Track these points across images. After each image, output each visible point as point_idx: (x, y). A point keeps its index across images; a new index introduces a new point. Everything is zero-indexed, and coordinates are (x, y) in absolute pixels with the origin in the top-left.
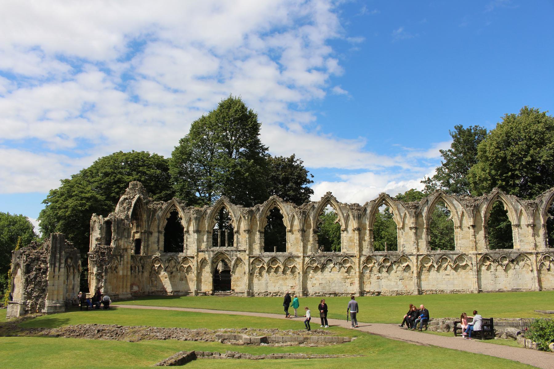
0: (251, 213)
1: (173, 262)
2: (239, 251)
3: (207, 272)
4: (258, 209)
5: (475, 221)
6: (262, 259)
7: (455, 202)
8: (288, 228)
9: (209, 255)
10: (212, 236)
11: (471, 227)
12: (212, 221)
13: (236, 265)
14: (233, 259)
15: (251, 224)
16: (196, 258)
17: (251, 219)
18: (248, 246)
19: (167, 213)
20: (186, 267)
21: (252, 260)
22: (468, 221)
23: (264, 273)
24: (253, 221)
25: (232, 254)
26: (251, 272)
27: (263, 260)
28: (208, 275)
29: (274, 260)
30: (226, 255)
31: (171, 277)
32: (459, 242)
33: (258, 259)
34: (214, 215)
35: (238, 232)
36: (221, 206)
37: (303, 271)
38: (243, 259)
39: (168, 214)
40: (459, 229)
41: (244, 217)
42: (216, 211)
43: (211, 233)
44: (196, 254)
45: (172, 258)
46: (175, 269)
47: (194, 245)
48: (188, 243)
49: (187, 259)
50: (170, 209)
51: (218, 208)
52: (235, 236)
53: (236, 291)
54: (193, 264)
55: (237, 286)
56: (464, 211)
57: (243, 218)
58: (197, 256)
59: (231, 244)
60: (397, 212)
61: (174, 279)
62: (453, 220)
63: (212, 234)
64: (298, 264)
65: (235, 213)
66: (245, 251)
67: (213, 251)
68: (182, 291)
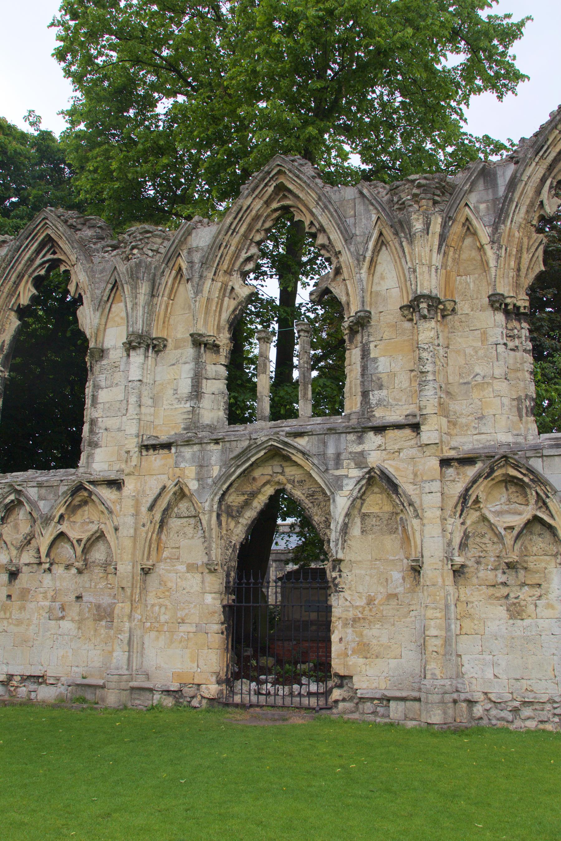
1: (21, 515)
2: (380, 429)
3: (191, 568)
6: (531, 471)
10: (224, 372)
12: (224, 286)
13: (358, 520)
14: (338, 484)
15: (444, 265)
17: (443, 238)
19: (17, 284)
20: (79, 541)
24: (458, 250)
25: (331, 451)
26: (459, 560)
27: (538, 479)
30: (298, 458)
31: (9, 596)
34: (236, 255)
36: (275, 205)
38: (399, 480)
39: (21, 288)
42: (245, 236)
43: (215, 348)
45: (19, 492)
46: (27, 557)
49: (91, 493)
50: (31, 260)
51: (257, 218)
61: (22, 608)
63: (223, 357)
65: (350, 221)
66: (416, 427)
68: (58, 679)
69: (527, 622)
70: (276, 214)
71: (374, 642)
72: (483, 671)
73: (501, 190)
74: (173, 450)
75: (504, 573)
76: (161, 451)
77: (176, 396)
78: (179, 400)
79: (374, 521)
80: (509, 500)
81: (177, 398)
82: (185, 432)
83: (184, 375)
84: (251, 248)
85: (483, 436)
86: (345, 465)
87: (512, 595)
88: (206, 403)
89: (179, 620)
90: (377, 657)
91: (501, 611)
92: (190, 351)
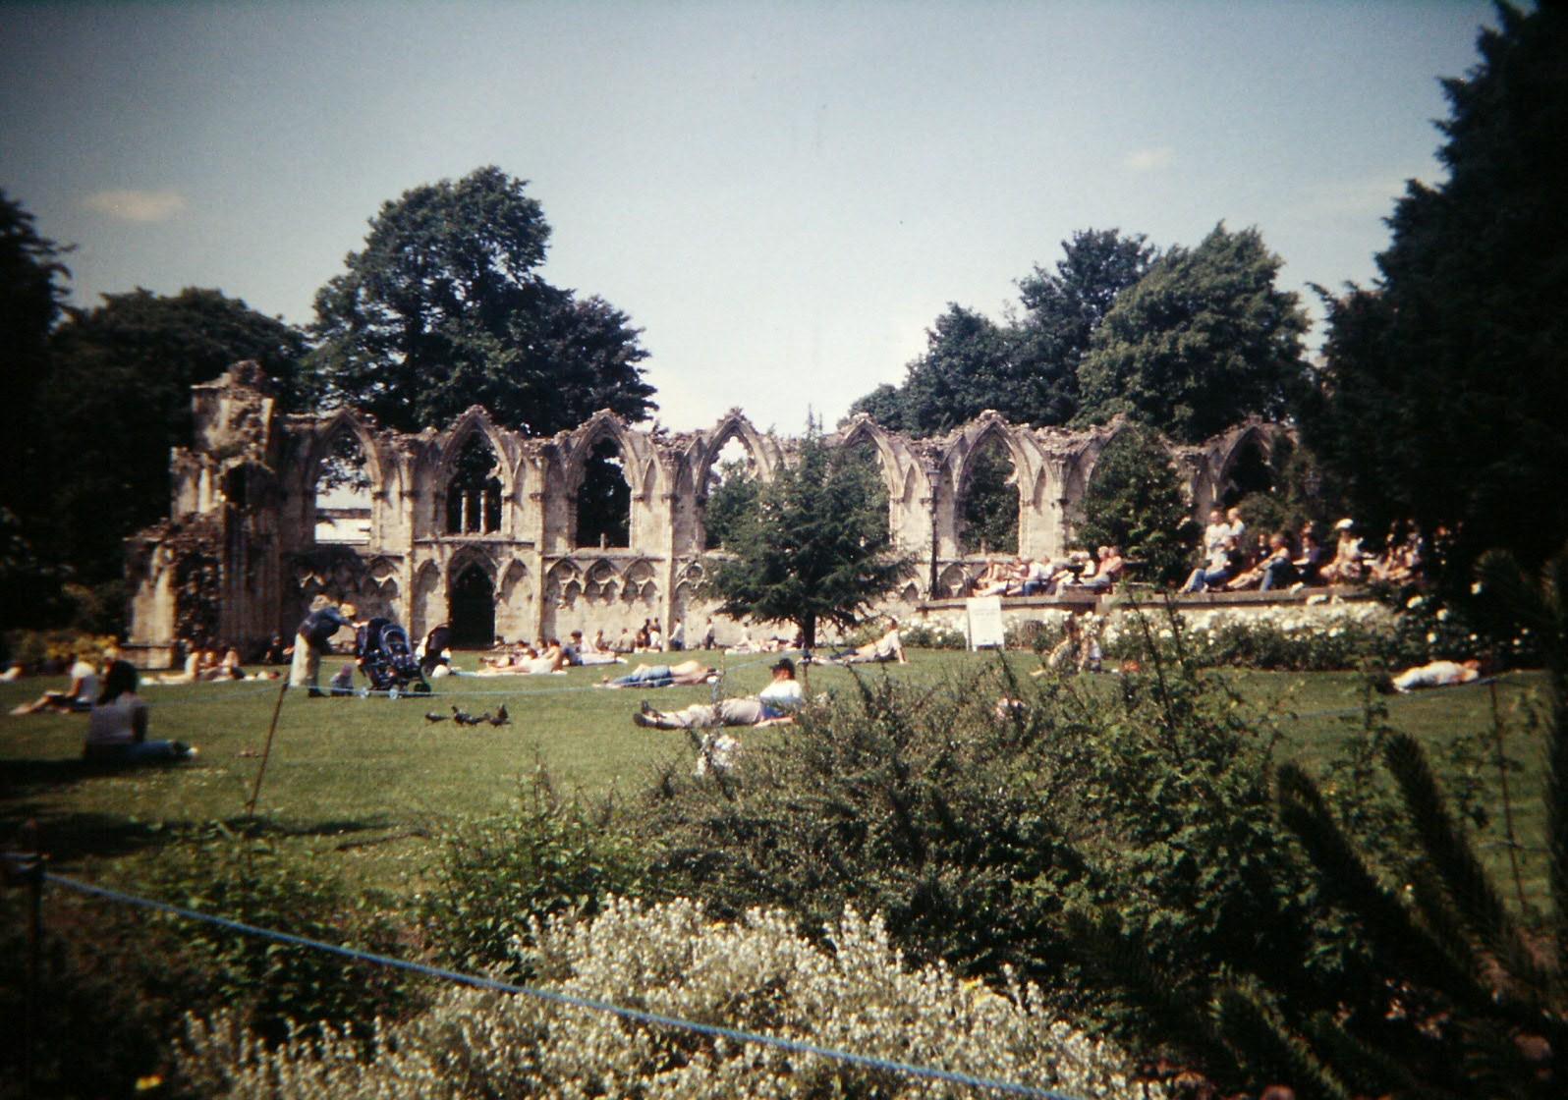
0: (549, 452)
4: (567, 444)
5: (1065, 492)
7: (1028, 447)
8: (636, 491)
9: (442, 553)
11: (1057, 504)
14: (500, 564)
16: (407, 560)
18: (540, 532)
21: (549, 567)
22: (1054, 490)
23: (579, 602)
27: (576, 568)
29: (603, 566)
32: (1029, 536)
33: (566, 565)
35: (514, 498)
37: (671, 594)
40: (1031, 508)
41: (533, 462)
44: (409, 550)
47: (401, 528)
48: (384, 522)
52: (506, 509)
53: (507, 640)
54: (402, 577)
55: (510, 627)
56: (1046, 467)
57: (528, 465)
58: (412, 555)
59: (494, 523)
60: (893, 461)
62: (1020, 486)
64: (662, 581)
67: (452, 544)
92: (431, 500)
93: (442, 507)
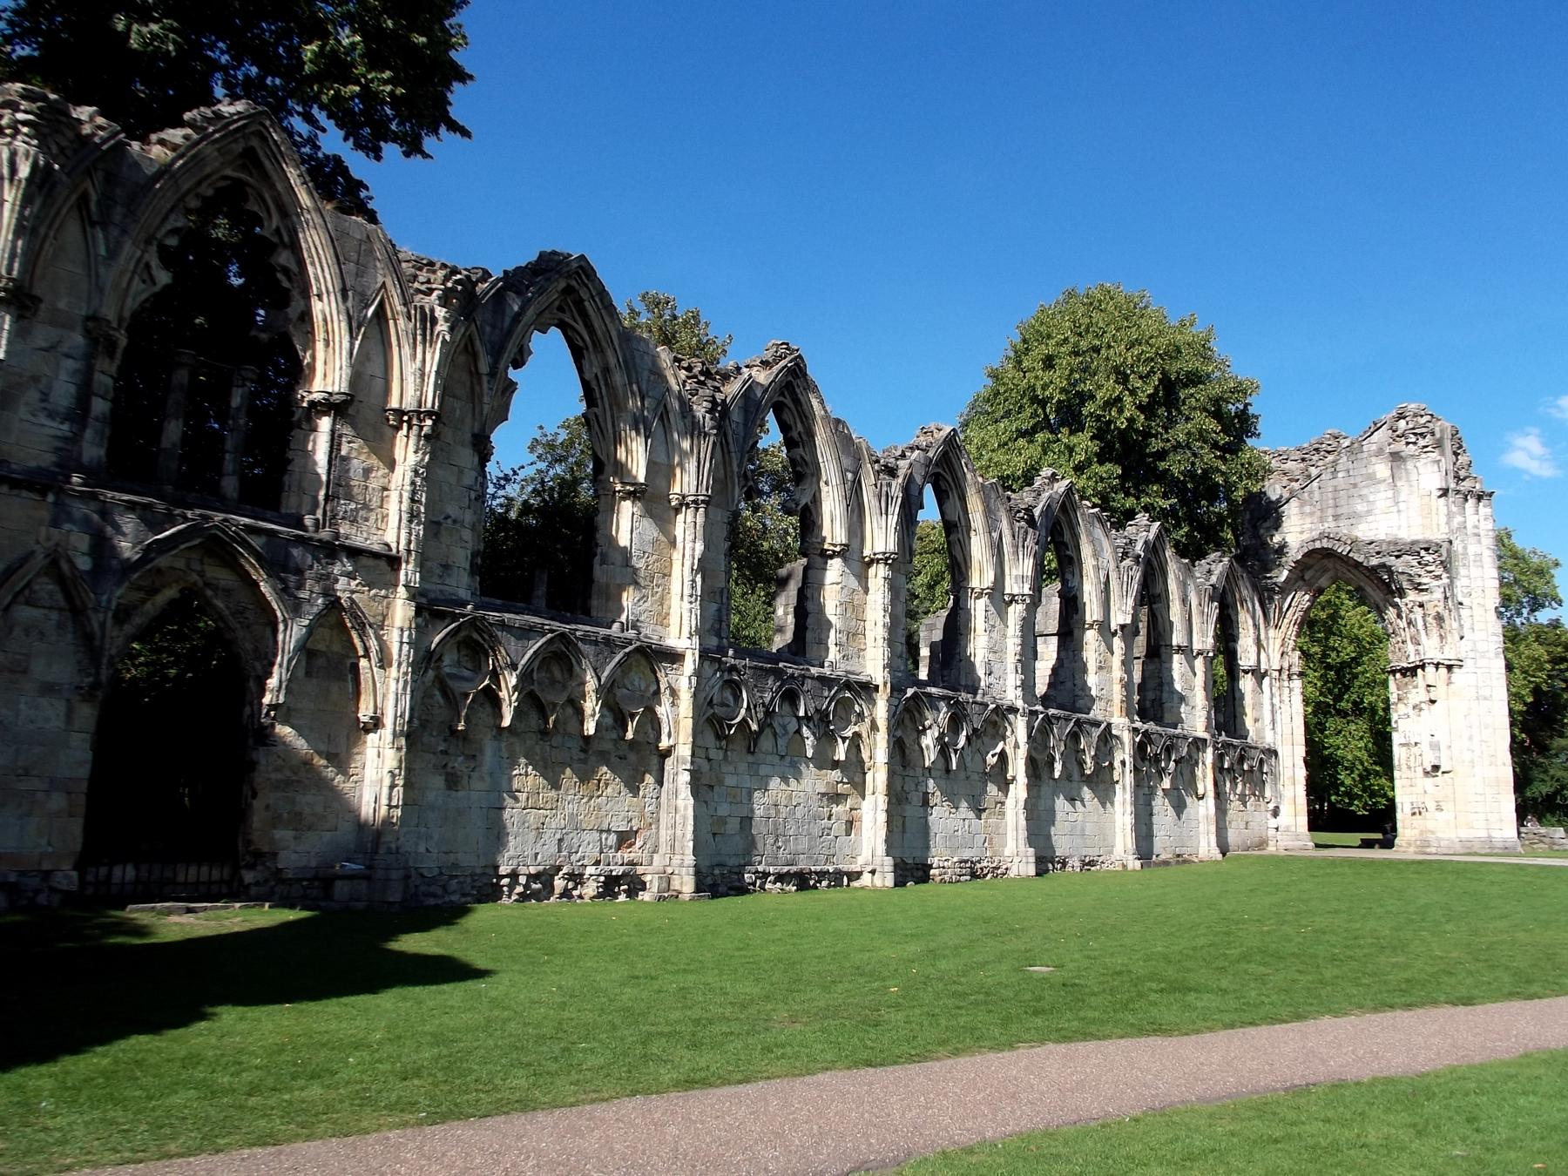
28: (51, 713)
36: (228, 172)
69: (460, 794)
70: (223, 184)
71: (307, 810)
72: (417, 844)
73: (508, 320)
74: (51, 498)
75: (445, 740)
76: (24, 493)
77: (43, 405)
78: (51, 415)
79: (321, 661)
80: (459, 662)
81: (45, 409)
82: (57, 470)
83: (63, 376)
84: (173, 217)
85: (447, 588)
86: (307, 587)
87: (450, 765)
88: (89, 434)
89: (20, 771)
90: (309, 829)
91: (438, 781)
92: (78, 340)
93: (105, 374)
